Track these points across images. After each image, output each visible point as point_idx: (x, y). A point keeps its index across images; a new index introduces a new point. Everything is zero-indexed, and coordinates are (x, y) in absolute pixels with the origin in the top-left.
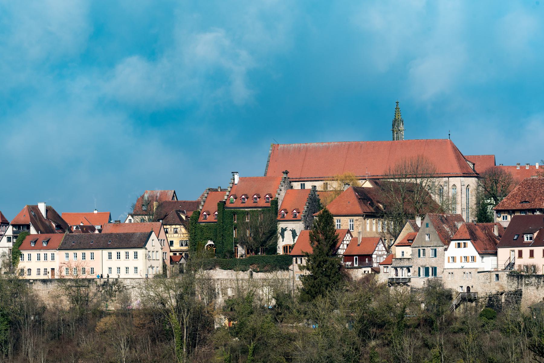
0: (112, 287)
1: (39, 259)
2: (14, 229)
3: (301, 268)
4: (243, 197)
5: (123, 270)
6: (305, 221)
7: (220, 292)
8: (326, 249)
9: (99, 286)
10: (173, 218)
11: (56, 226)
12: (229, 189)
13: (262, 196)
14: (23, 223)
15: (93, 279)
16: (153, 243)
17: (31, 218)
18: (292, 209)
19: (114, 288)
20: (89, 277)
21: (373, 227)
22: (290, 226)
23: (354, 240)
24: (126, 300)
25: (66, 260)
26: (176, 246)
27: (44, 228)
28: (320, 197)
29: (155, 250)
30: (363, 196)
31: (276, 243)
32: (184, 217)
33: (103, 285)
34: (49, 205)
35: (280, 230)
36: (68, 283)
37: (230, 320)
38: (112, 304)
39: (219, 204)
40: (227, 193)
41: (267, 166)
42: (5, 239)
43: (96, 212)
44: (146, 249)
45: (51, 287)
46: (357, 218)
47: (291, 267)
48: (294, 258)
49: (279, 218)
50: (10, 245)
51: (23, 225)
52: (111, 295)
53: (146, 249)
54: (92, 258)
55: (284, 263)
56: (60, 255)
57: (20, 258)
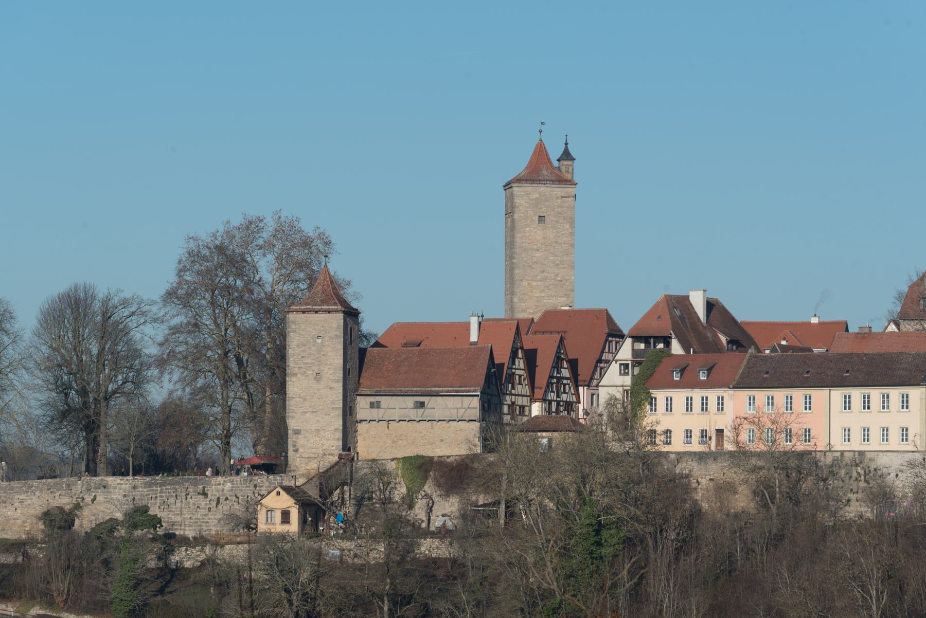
1: (689, 407)
5: (876, 435)
11: (728, 343)
15: (810, 453)
34: (712, 295)
36: (753, 461)
42: (614, 368)
50: (627, 380)
57: (648, 407)
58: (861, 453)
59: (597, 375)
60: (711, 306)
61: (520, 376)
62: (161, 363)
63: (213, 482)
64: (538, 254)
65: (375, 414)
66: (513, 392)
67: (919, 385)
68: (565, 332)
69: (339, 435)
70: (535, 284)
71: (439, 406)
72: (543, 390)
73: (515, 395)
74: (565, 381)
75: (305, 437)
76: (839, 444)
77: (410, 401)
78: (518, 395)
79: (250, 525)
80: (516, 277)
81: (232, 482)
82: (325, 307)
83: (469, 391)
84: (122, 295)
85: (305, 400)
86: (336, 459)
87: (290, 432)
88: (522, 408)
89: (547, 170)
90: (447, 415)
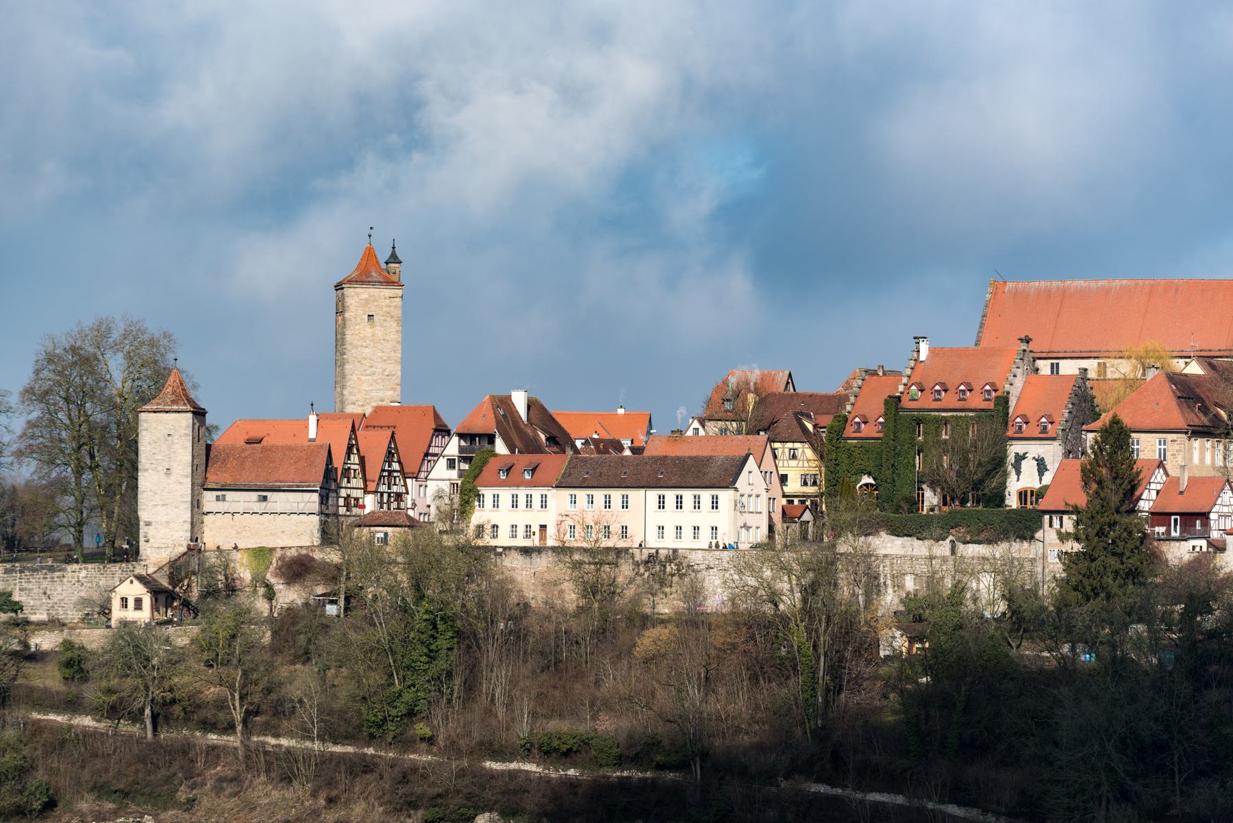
0: (663, 567)
1: (515, 505)
2: (463, 443)
3: (1063, 537)
4: (938, 388)
5: (687, 532)
6: (1065, 441)
7: (889, 582)
8: (1115, 499)
9: (637, 564)
10: (789, 427)
11: (548, 439)
12: (909, 372)
13: (977, 387)
14: (481, 432)
15: (627, 550)
16: (751, 478)
18: (1039, 415)
19: (668, 569)
20: (621, 544)
21: (1204, 456)
22: (1034, 449)
23: (1172, 482)
24: (695, 593)
25: (568, 508)
26: (794, 486)
27: (523, 443)
28: (1094, 392)
29: (754, 493)
30: (1186, 391)
31: (1003, 486)
32: (810, 426)
33: (647, 562)
34: (533, 396)
35: (1011, 458)
36: (577, 557)
37: (912, 641)
38: (665, 601)
39: (886, 402)
40: (905, 380)
41: (982, 325)
42: (442, 462)
43: (621, 411)
44: (736, 489)
45: (542, 563)
46: (1174, 436)
47: (1039, 535)
48: (1047, 517)
49: (1010, 433)
50: (454, 474)
51: (480, 435)
52: (662, 583)
53: (736, 489)
54: (625, 505)
55: (1024, 524)
56: (559, 499)
57: (477, 503)
58: (675, 551)
59: (424, 468)
62: (19, 454)
64: (367, 350)
65: (221, 506)
69: (188, 526)
71: (279, 500)
76: (653, 542)
77: (254, 496)
79: (105, 611)
81: (86, 569)
82: (175, 407)
86: (184, 549)
87: (141, 523)
88: (357, 499)
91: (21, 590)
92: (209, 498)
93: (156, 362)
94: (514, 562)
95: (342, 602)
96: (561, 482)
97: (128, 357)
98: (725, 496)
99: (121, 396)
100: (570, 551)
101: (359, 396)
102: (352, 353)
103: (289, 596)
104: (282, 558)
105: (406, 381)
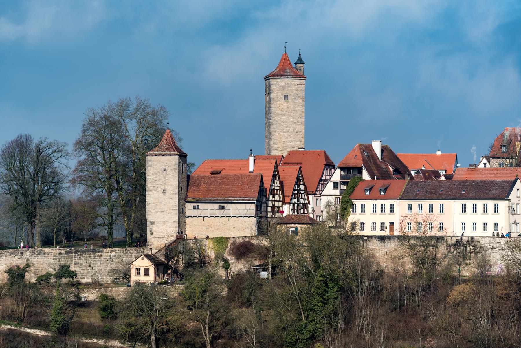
0: (465, 248)
1: (374, 210)
2: (343, 173)
5: (480, 227)
9: (449, 246)
11: (394, 171)
14: (354, 166)
15: (443, 237)
17: (364, 159)
19: (468, 249)
20: (439, 234)
24: (485, 263)
25: (407, 212)
33: (455, 245)
36: (412, 242)
38: (466, 268)
42: (330, 185)
43: (439, 153)
44: (509, 200)
45: (391, 245)
50: (337, 192)
51: (353, 169)
52: (465, 257)
53: (509, 200)
54: (442, 210)
56: (401, 206)
57: (351, 210)
58: (472, 238)
59: (319, 189)
60: (384, 150)
61: (277, 190)
63: (104, 251)
64: (284, 117)
65: (196, 212)
66: (274, 199)
67: (504, 199)
68: (301, 164)
69: (177, 225)
70: (282, 134)
71: (232, 209)
72: (290, 198)
73: (275, 201)
74: (302, 192)
75: (157, 226)
77: (216, 206)
78: (276, 201)
79: (127, 276)
80: (272, 130)
82: (168, 152)
83: (249, 200)
84: (49, 141)
85: (157, 205)
86: (174, 239)
88: (278, 208)
89: (289, 69)
90: (237, 213)
91: (75, 264)
92: (189, 208)
93: (156, 125)
94: (374, 246)
95: (270, 270)
96: (402, 197)
97: (139, 122)
98: (503, 204)
99: (135, 145)
100: (409, 238)
101: (280, 145)
102: (275, 119)
103: (238, 266)
104: (233, 244)
105: (308, 136)
